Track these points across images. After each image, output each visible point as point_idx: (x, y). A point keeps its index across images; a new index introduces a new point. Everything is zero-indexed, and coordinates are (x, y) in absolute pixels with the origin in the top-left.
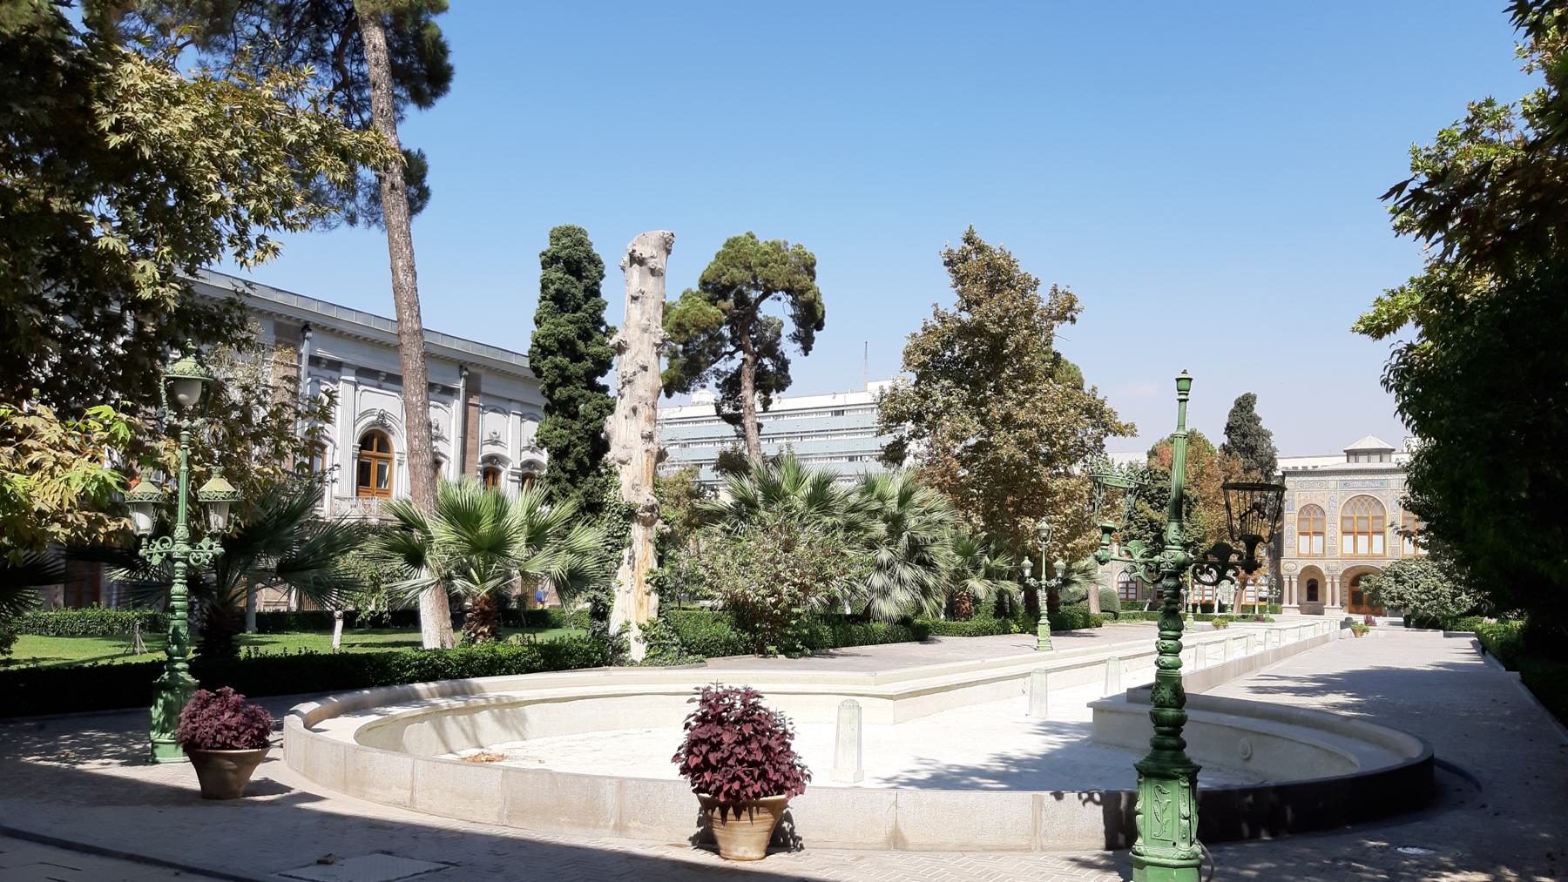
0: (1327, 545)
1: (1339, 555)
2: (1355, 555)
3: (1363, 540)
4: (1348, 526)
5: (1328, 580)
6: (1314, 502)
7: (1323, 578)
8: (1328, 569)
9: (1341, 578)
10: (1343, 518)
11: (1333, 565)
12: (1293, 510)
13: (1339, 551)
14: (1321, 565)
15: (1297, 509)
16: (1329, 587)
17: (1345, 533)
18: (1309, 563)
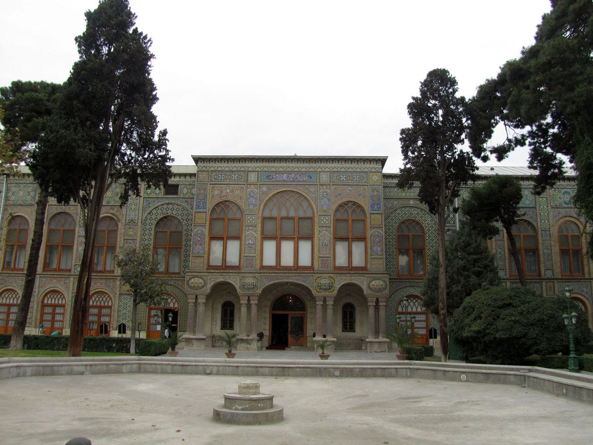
0: (242, 256)
1: (258, 267)
2: (278, 267)
3: (287, 247)
4: (270, 227)
5: (244, 301)
6: (230, 198)
7: (237, 297)
8: (243, 286)
9: (261, 297)
10: (264, 219)
11: (250, 280)
12: (205, 207)
13: (258, 262)
14: (234, 280)
15: (210, 206)
16: (244, 310)
17: (265, 237)
18: (221, 279)
